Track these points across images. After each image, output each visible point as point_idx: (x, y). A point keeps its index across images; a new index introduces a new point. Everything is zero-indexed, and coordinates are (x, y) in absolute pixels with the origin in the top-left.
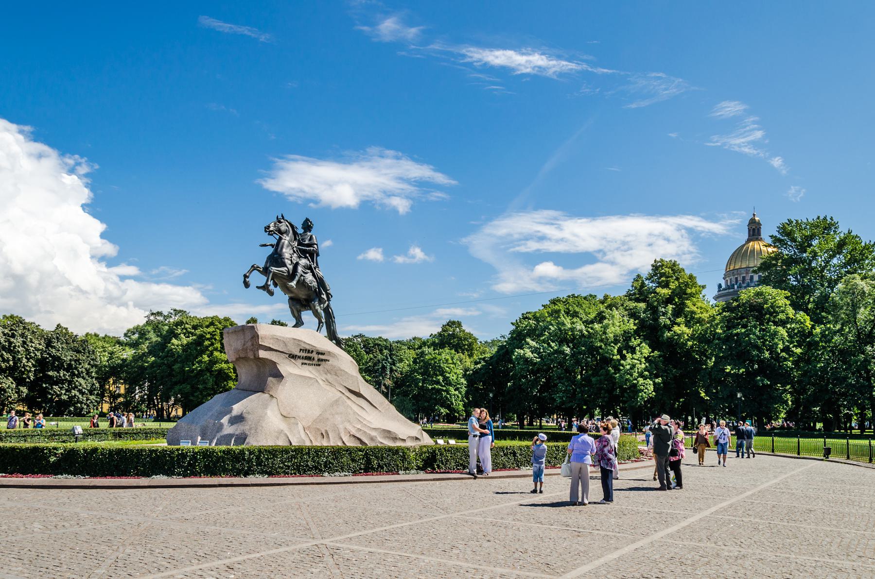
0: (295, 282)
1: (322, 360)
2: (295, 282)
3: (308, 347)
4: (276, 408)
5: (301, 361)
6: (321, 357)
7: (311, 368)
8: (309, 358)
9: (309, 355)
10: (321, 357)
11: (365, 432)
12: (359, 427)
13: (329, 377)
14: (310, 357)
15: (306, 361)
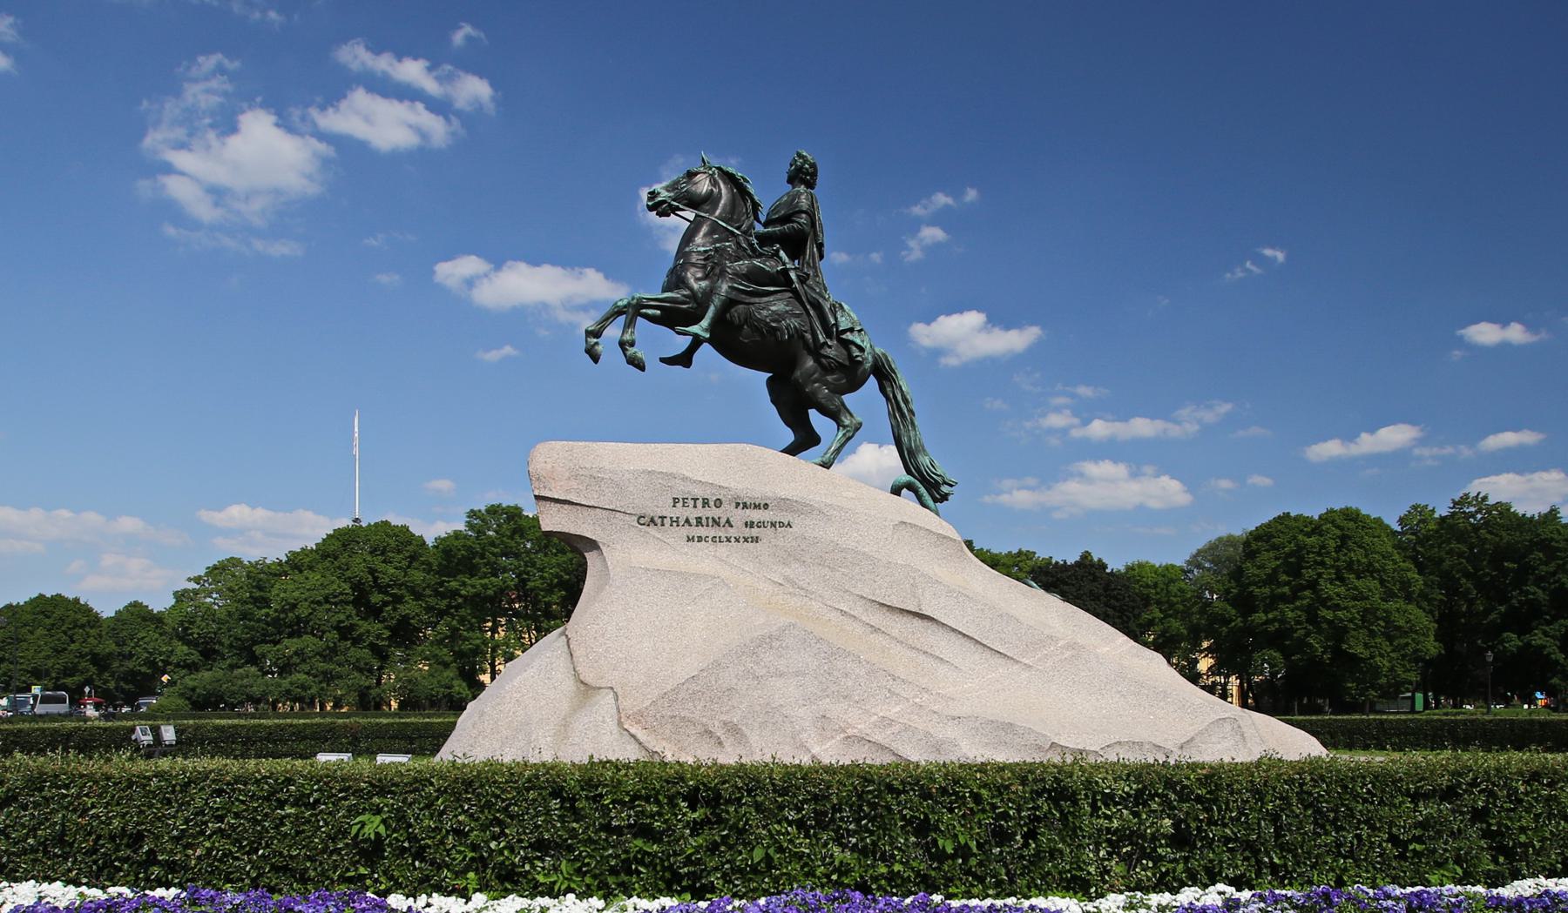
0: (705, 323)
1: (761, 525)
2: (705, 323)
3: (698, 492)
4: (562, 663)
5: (685, 531)
6: (756, 515)
7: (723, 549)
8: (716, 522)
9: (712, 512)
10: (756, 515)
11: (907, 728)
12: (894, 711)
13: (793, 571)
14: (707, 517)
15: (702, 531)
